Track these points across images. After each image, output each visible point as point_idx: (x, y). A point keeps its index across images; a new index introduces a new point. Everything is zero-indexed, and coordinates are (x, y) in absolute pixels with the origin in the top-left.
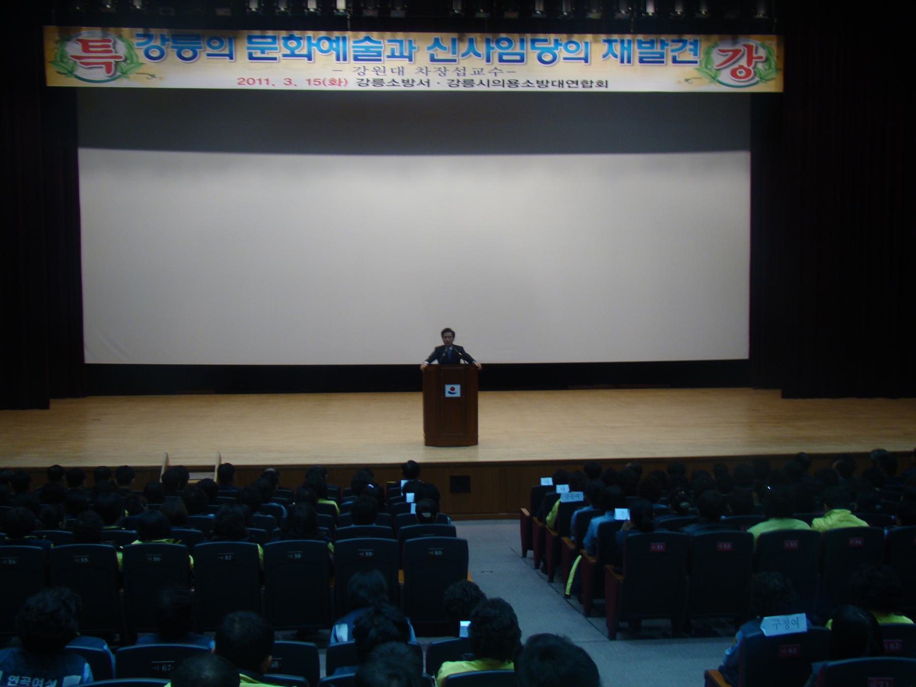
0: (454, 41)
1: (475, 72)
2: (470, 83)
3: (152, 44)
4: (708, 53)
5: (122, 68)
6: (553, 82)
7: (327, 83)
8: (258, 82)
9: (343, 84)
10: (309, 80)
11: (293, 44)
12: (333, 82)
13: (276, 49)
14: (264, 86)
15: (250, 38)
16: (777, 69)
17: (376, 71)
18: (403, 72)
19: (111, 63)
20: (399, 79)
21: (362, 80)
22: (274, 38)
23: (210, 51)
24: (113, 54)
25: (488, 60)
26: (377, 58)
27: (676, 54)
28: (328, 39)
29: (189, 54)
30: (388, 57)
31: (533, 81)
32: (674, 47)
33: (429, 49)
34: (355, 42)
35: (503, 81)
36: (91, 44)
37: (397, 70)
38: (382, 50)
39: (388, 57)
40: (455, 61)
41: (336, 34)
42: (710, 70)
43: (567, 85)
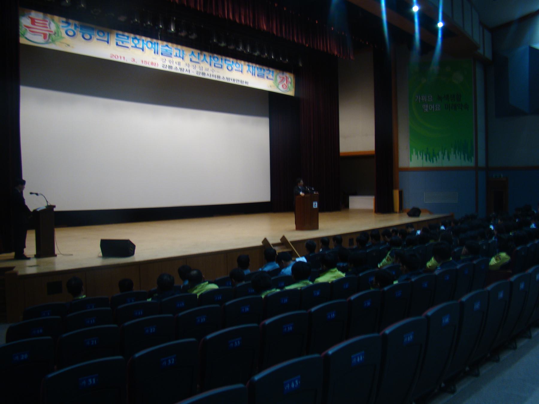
0: (199, 54)
3: (70, 28)
4: (276, 77)
5: (52, 38)
7: (150, 63)
8: (119, 58)
11: (136, 41)
12: (152, 63)
14: (122, 60)
15: (117, 35)
16: (293, 87)
17: (170, 62)
20: (178, 67)
22: (128, 37)
23: (98, 37)
24: (49, 29)
25: (210, 65)
26: (170, 55)
28: (151, 43)
29: (87, 37)
37: (178, 64)
41: (155, 41)
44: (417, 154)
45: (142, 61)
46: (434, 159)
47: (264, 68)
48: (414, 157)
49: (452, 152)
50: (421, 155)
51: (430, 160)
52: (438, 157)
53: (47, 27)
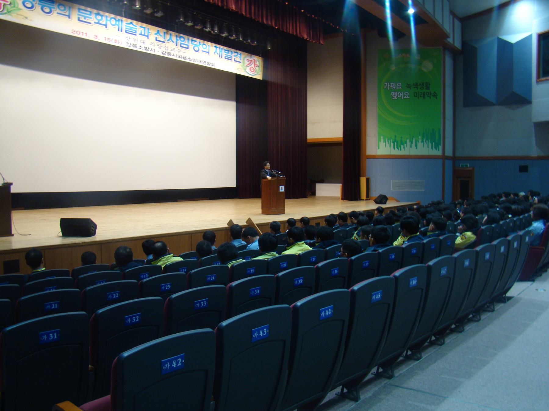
0: (164, 32)
2: (169, 54)
4: (244, 60)
9: (120, 43)
10: (105, 38)
11: (99, 17)
12: (116, 41)
13: (91, 18)
14: (84, 37)
15: (79, 9)
20: (143, 46)
22: (91, 12)
25: (176, 45)
27: (235, 57)
28: (115, 19)
29: (47, 10)
31: (191, 58)
33: (155, 34)
34: (126, 24)
35: (181, 56)
38: (137, 30)
40: (164, 42)
41: (119, 17)
42: (244, 66)
44: (385, 141)
46: (402, 146)
47: (232, 50)
48: (382, 144)
49: (420, 141)
50: (389, 142)
51: (398, 149)
52: (405, 145)
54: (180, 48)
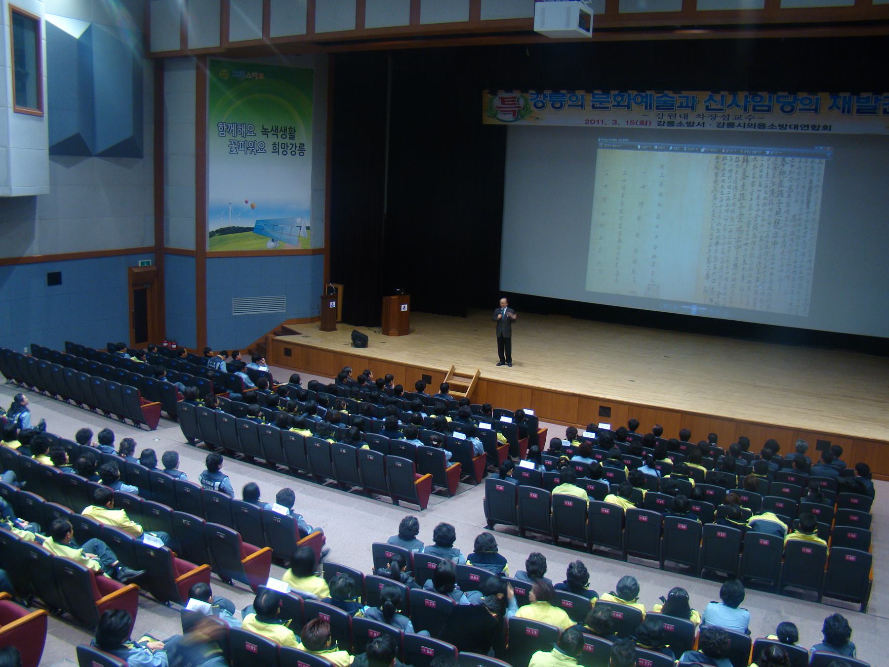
1: (736, 119)
6: (790, 126)
7: (638, 123)
9: (648, 124)
17: (670, 116)
18: (687, 117)
19: (516, 111)
20: (684, 122)
21: (661, 122)
24: (517, 105)
25: (745, 110)
26: (670, 107)
30: (678, 107)
31: (777, 125)
32: (886, 102)
36: (506, 100)
37: (683, 116)
39: (678, 107)
40: (722, 110)
43: (801, 128)
45: (628, 121)
53: (516, 104)
54: (751, 112)
